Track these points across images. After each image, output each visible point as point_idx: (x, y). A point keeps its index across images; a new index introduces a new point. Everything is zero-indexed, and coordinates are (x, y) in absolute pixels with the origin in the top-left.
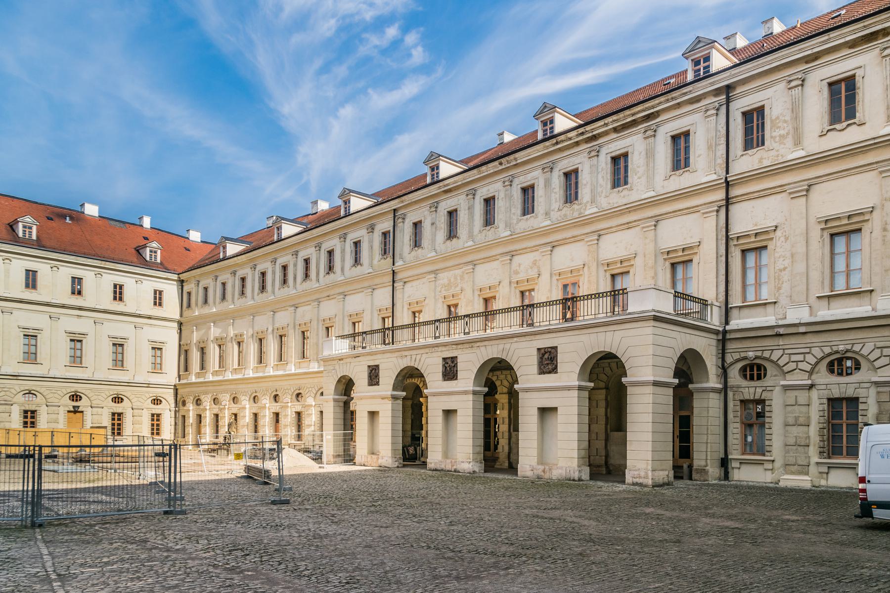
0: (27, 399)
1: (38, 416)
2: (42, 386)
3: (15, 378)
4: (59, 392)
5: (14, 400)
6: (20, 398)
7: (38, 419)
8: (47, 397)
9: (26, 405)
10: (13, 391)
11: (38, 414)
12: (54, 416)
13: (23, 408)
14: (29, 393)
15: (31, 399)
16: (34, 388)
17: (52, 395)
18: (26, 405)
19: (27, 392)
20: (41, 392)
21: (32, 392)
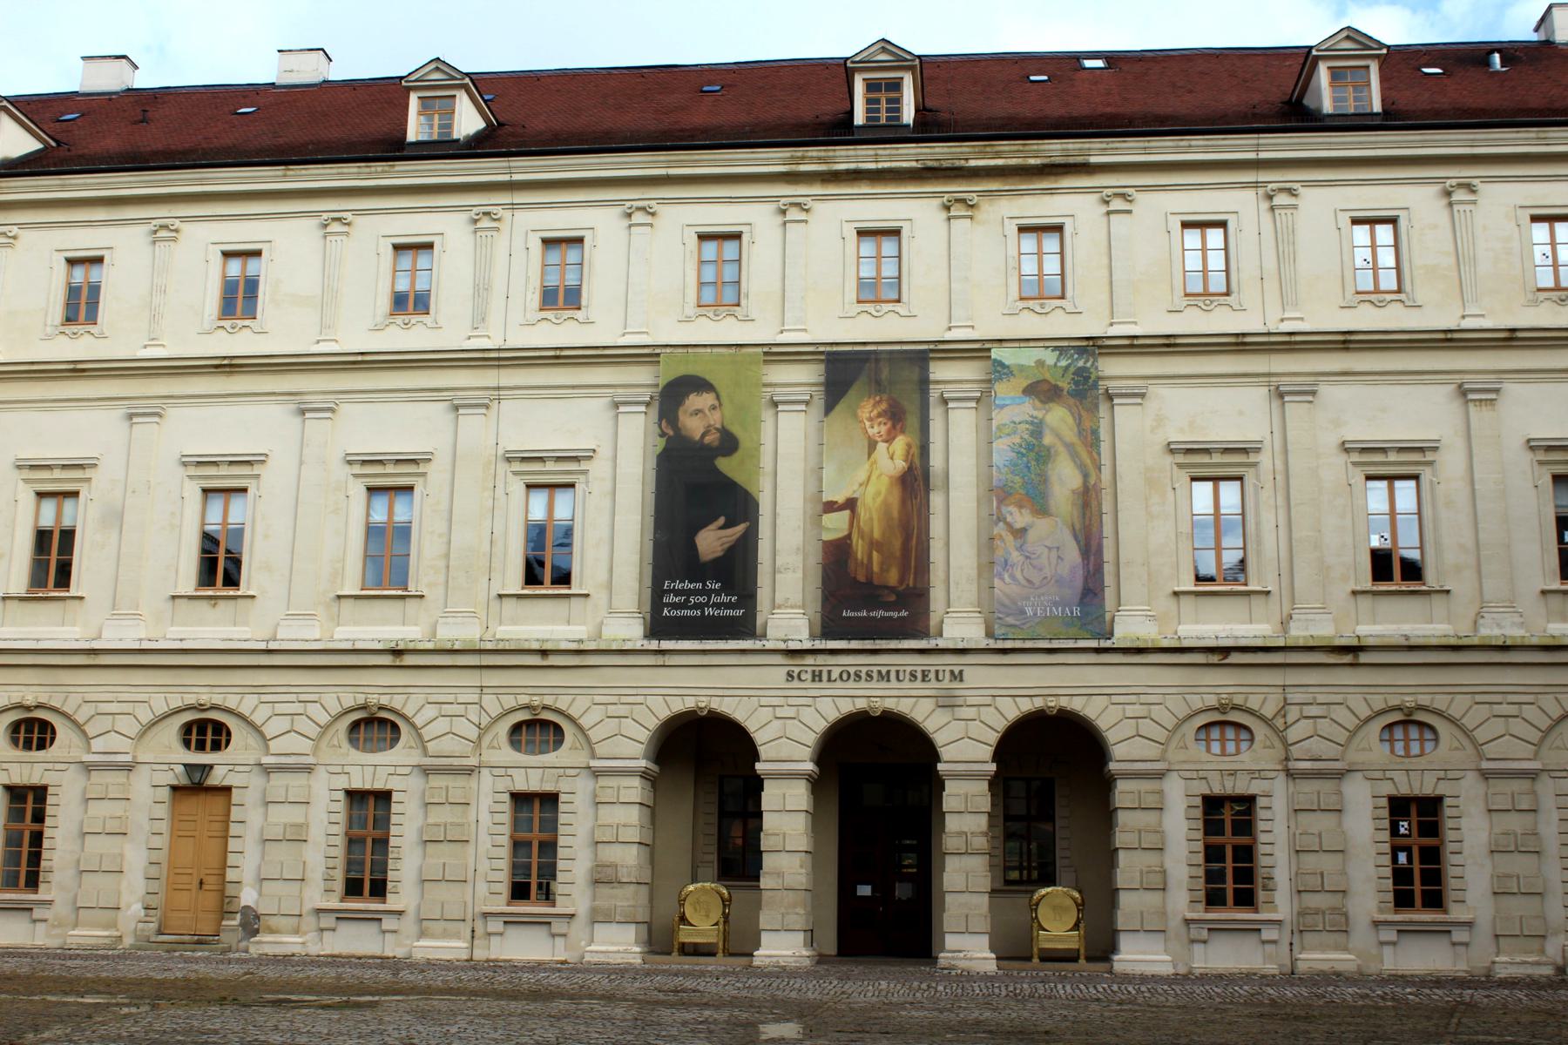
0: (1399, 746)
1: (1449, 823)
2: (1453, 690)
3: (1348, 659)
4: (1529, 712)
5: (1354, 756)
6: (1372, 749)
7: (1450, 835)
8: (1480, 735)
9: (1400, 777)
10: (1341, 714)
11: (1448, 812)
12: (1516, 823)
13: (1388, 789)
14: (1405, 723)
15: (1415, 748)
16: (1424, 700)
17: (1498, 726)
18: (1400, 777)
19: (1398, 717)
20: (1455, 712)
21: (1420, 716)
